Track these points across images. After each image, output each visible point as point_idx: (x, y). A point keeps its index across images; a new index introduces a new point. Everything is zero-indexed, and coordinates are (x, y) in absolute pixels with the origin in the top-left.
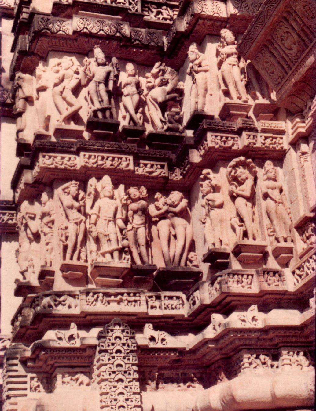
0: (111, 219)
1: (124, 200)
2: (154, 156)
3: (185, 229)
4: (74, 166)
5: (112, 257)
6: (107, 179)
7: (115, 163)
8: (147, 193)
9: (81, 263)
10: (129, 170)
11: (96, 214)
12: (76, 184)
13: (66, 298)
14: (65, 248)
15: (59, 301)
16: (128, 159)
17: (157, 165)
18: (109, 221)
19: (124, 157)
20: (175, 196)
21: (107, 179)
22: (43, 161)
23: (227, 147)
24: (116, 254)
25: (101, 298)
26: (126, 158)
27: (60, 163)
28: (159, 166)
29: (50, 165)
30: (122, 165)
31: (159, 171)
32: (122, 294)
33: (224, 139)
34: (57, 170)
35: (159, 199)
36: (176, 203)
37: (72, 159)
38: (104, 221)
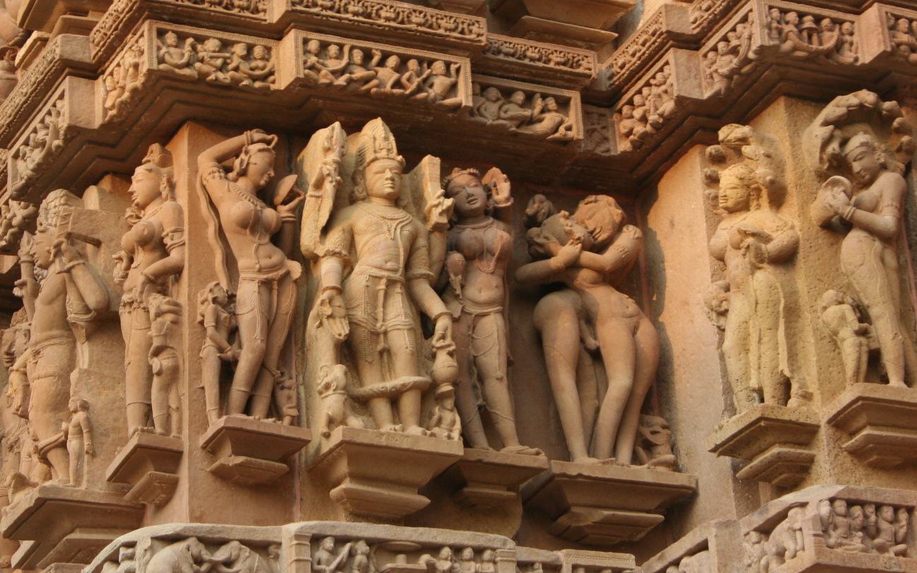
0: (398, 276)
1: (441, 214)
2: (541, 64)
3: (634, 331)
4: (264, 78)
6: (376, 132)
7: (409, 80)
8: (513, 192)
9: (282, 428)
10: (457, 108)
11: (334, 254)
12: (268, 143)
13: (235, 553)
14: (227, 369)
15: (210, 561)
16: (453, 67)
17: (544, 96)
19: (440, 60)
20: (601, 211)
21: (376, 132)
22: (159, 49)
23: (818, 53)
24: (409, 403)
25: (360, 558)
26: (448, 65)
27: (219, 62)
28: (552, 103)
29: (181, 67)
30: (431, 86)
31: (549, 120)
32: (434, 549)
33: (808, 22)
34: (202, 87)
35: (540, 218)
36: (603, 237)
37: (258, 51)
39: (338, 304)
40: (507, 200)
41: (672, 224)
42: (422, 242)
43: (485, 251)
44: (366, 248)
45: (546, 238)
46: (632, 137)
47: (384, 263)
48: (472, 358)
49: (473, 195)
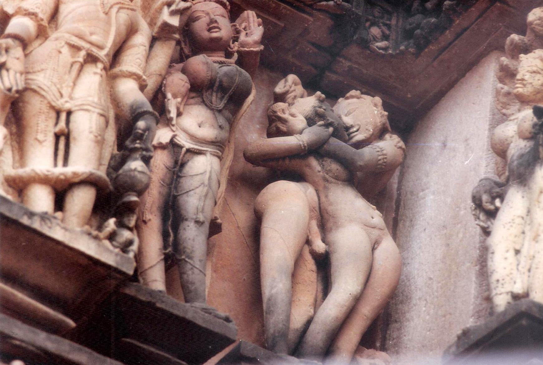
5: (60, 203)
18: (91, 59)
24: (82, 200)
38: (66, 50)
39: (17, 56)
40: (256, 43)
41: (444, 145)
42: (141, 40)
43: (217, 84)
44: (70, 16)
45: (293, 115)
46: (418, 31)
47: (88, 33)
48: (171, 198)
49: (216, 22)
